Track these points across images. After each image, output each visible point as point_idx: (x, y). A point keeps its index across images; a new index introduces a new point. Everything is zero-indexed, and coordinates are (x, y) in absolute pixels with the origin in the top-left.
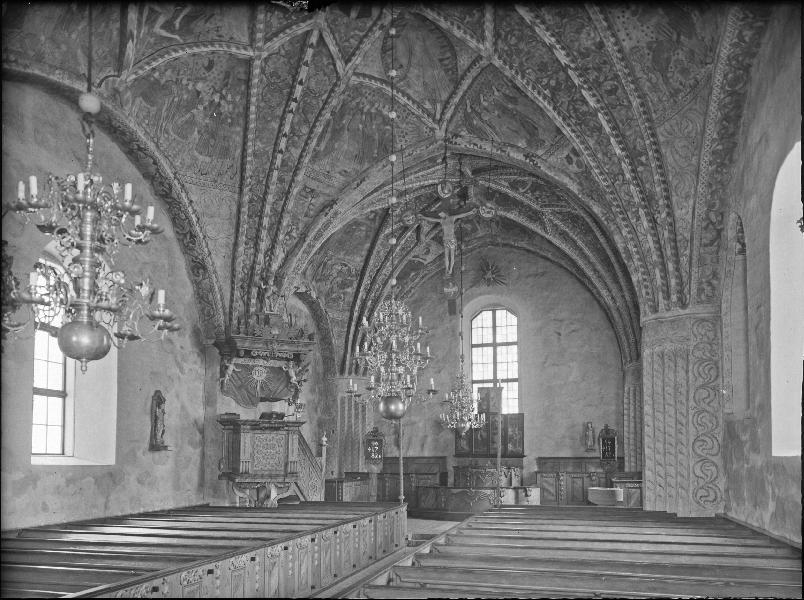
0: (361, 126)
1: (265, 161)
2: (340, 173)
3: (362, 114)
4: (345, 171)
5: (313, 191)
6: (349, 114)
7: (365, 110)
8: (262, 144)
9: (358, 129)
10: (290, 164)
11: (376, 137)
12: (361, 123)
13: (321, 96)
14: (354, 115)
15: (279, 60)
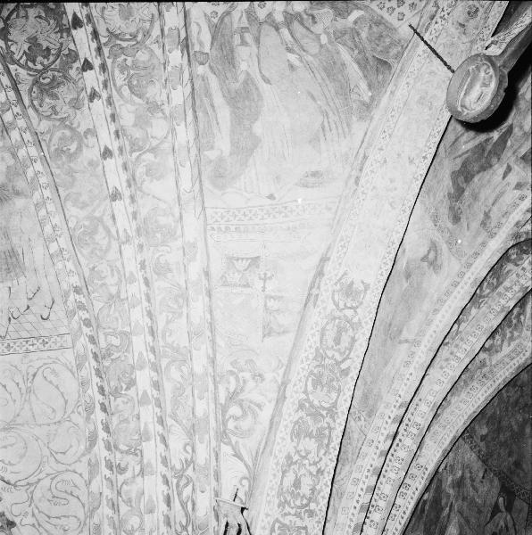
0: (293, 58)
1: (105, 242)
2: (306, 186)
3: (277, 29)
4: (315, 174)
5: (255, 261)
6: (244, 43)
7: (279, 18)
8: (84, 206)
9: (292, 67)
10: (163, 220)
11: (346, 55)
12: (289, 50)
13: (147, 34)
14: (257, 40)
15: (26, 17)
